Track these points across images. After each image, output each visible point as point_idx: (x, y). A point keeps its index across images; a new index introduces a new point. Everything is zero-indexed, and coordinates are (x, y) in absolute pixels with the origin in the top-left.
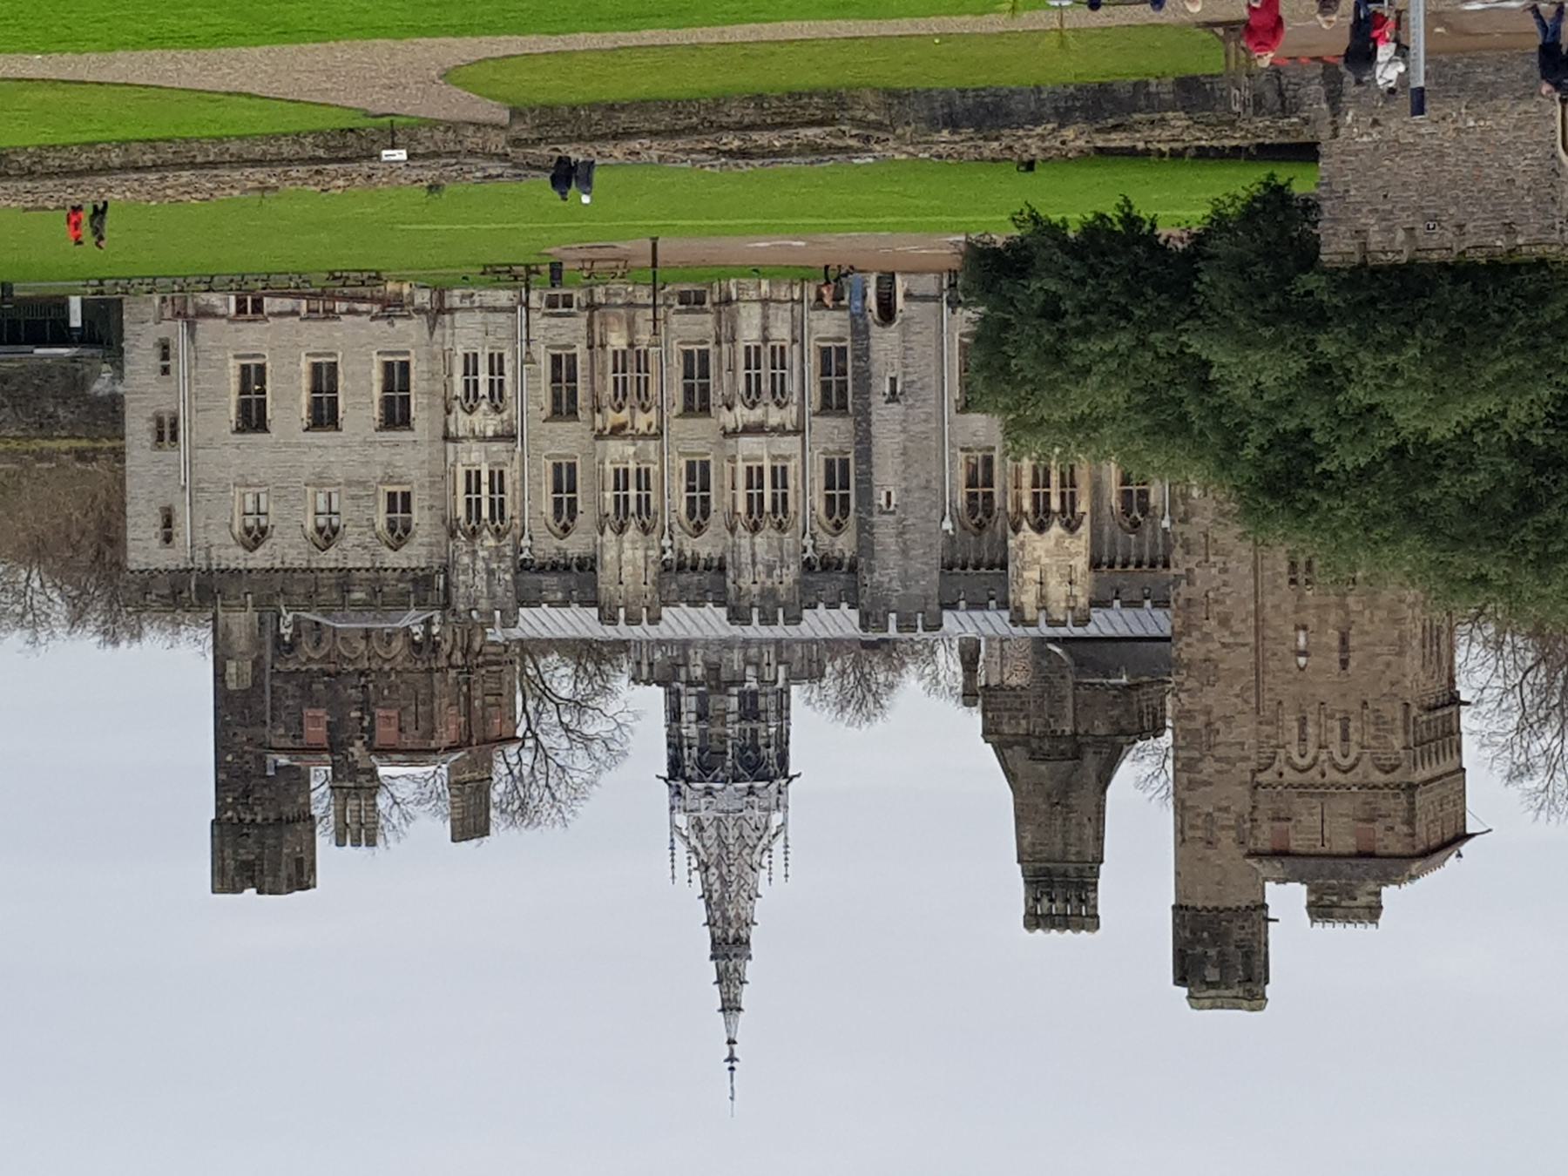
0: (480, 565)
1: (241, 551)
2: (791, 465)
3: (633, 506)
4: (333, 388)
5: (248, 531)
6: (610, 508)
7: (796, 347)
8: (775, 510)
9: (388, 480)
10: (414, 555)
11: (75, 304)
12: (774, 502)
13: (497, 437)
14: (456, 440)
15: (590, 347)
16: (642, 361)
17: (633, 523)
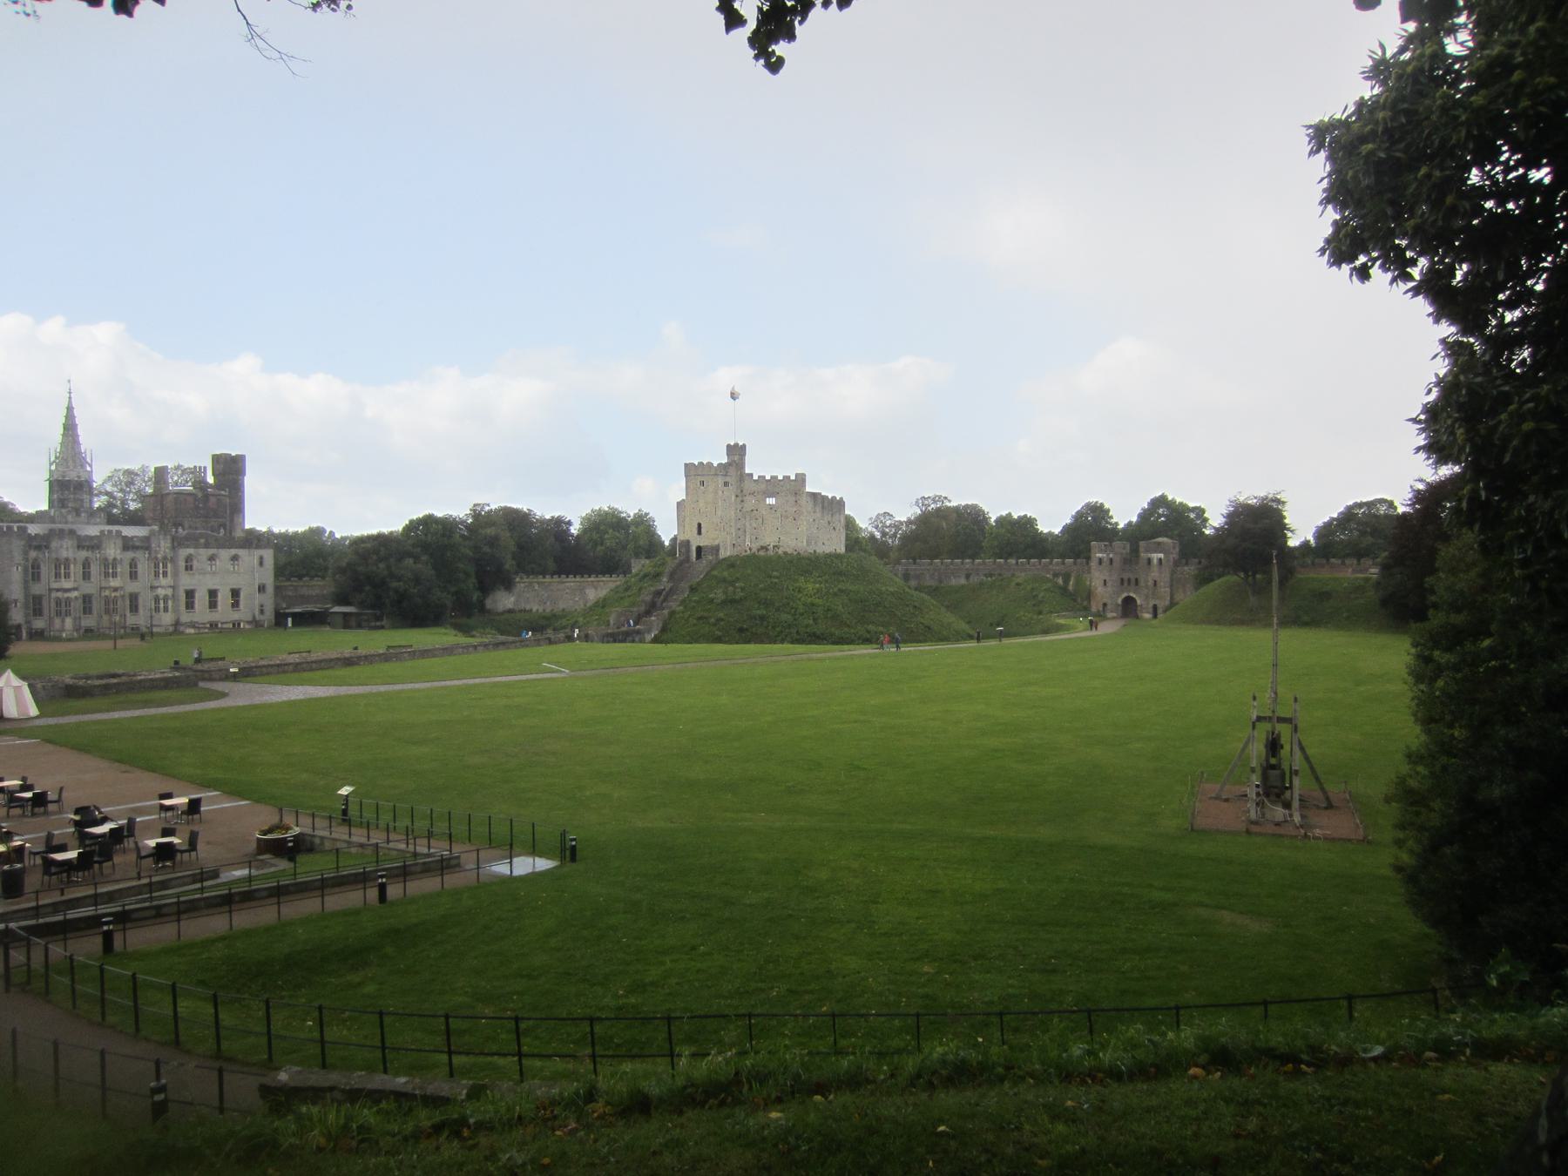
0: (163, 549)
1: (240, 554)
2: (53, 579)
3: (111, 567)
4: (210, 602)
5: (237, 560)
6: (119, 566)
7: (52, 615)
8: (60, 565)
9: (193, 574)
10: (184, 553)
11: (290, 625)
12: (60, 567)
13: (158, 587)
14: (171, 587)
15: (125, 615)
16: (107, 611)
17: (110, 561)
